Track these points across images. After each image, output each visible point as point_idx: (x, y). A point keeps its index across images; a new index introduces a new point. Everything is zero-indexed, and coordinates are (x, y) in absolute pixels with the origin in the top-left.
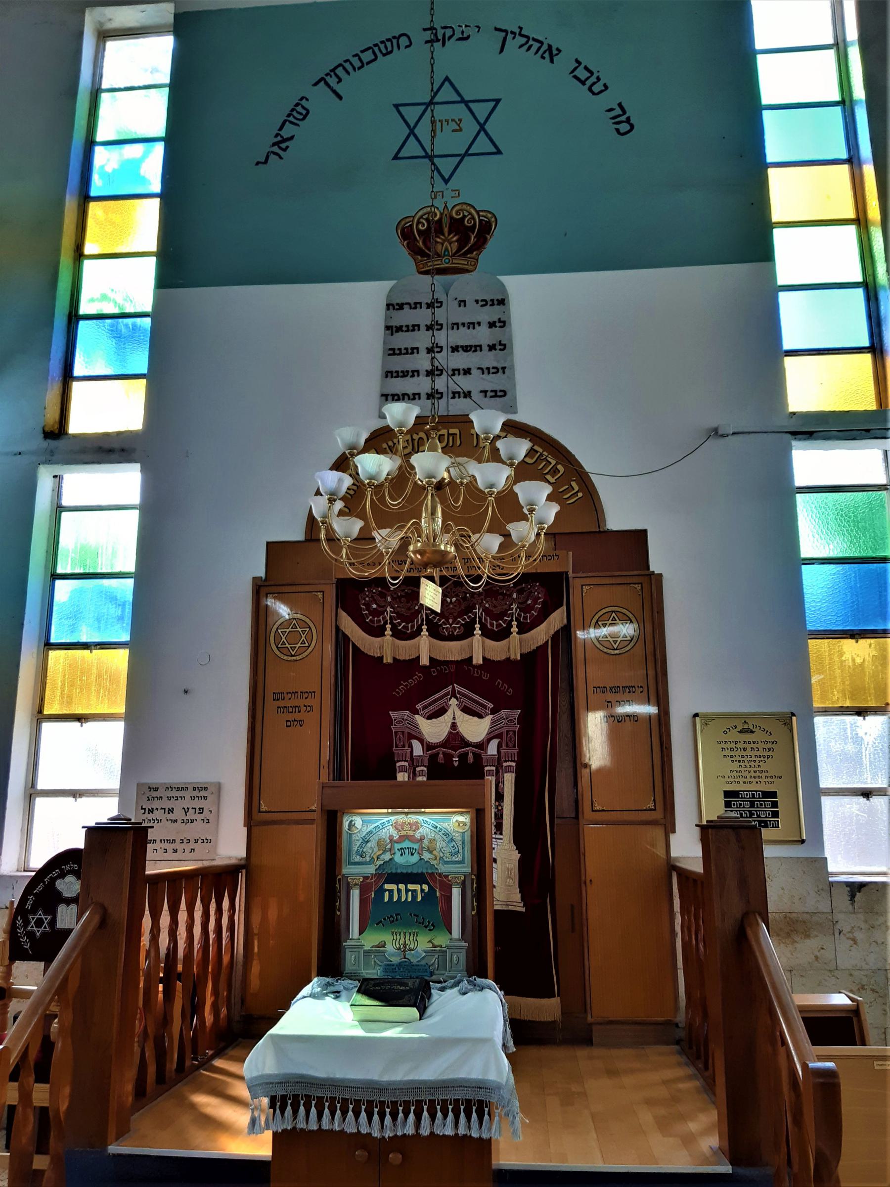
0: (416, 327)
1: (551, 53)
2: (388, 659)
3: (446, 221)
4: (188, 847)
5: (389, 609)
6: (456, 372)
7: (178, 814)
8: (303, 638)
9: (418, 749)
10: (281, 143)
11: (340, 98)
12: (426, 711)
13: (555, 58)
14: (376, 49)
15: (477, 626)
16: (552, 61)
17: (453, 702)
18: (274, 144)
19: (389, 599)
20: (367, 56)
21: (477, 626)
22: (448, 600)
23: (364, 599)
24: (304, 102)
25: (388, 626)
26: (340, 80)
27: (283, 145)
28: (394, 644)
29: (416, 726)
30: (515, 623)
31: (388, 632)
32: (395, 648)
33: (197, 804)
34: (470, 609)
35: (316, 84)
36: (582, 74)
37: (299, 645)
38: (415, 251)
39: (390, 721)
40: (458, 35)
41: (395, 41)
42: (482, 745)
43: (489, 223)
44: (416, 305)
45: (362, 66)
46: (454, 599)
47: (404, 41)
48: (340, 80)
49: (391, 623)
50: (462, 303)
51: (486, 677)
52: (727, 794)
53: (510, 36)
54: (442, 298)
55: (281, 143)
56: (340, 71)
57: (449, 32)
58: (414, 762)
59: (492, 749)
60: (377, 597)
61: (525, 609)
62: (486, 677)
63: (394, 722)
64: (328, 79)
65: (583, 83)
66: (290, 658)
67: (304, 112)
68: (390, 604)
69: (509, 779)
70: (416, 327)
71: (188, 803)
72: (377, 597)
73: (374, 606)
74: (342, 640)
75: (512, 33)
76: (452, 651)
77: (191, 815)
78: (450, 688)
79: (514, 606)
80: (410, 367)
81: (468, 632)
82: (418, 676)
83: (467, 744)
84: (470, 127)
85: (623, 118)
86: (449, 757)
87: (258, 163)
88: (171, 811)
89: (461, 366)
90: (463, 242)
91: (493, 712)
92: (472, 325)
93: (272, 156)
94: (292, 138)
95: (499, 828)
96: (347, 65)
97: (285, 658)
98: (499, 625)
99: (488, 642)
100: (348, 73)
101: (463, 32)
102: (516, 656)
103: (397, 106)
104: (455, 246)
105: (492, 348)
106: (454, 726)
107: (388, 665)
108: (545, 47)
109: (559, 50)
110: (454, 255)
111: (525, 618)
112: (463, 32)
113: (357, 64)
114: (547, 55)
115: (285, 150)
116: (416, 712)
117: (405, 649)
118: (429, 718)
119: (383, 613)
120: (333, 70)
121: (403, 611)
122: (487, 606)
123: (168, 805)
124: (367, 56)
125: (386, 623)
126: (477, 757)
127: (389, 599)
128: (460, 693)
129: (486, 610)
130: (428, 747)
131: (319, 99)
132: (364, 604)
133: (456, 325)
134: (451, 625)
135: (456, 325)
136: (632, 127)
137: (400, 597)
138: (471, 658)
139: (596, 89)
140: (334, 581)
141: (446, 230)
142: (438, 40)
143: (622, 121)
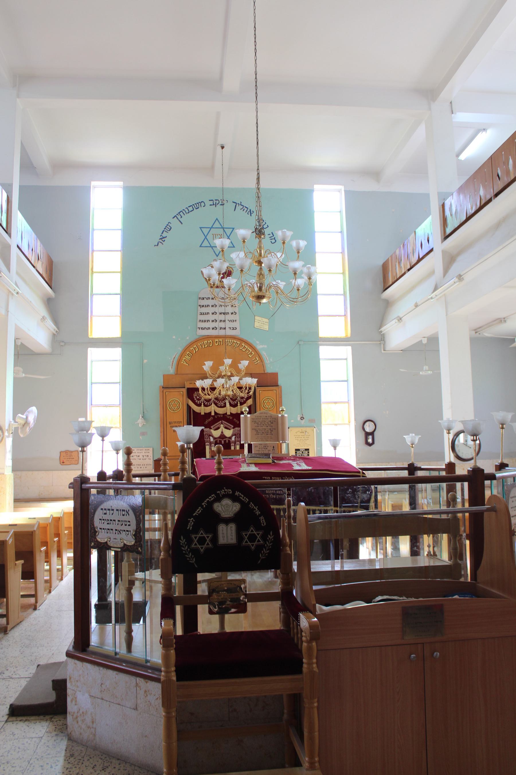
0: (208, 306)
2: (203, 413)
4: (144, 467)
6: (221, 321)
7: (141, 457)
10: (163, 238)
17: (222, 425)
20: (190, 209)
24: (169, 224)
27: (163, 240)
31: (202, 405)
32: (204, 410)
33: (147, 454)
35: (174, 218)
40: (220, 203)
42: (230, 438)
44: (208, 298)
47: (203, 204)
51: (231, 418)
52: (296, 450)
53: (237, 205)
55: (163, 238)
56: (181, 213)
57: (217, 202)
58: (211, 443)
62: (231, 418)
70: (208, 306)
76: (221, 411)
77: (145, 457)
82: (211, 418)
83: (226, 437)
88: (139, 456)
91: (233, 428)
93: (159, 243)
96: (184, 211)
99: (232, 408)
105: (232, 313)
106: (222, 432)
108: (249, 210)
113: (187, 212)
114: (249, 213)
115: (164, 241)
116: (211, 429)
117: (207, 410)
118: (215, 430)
123: (138, 454)
124: (190, 209)
126: (229, 441)
130: (215, 438)
131: (175, 223)
138: (226, 413)
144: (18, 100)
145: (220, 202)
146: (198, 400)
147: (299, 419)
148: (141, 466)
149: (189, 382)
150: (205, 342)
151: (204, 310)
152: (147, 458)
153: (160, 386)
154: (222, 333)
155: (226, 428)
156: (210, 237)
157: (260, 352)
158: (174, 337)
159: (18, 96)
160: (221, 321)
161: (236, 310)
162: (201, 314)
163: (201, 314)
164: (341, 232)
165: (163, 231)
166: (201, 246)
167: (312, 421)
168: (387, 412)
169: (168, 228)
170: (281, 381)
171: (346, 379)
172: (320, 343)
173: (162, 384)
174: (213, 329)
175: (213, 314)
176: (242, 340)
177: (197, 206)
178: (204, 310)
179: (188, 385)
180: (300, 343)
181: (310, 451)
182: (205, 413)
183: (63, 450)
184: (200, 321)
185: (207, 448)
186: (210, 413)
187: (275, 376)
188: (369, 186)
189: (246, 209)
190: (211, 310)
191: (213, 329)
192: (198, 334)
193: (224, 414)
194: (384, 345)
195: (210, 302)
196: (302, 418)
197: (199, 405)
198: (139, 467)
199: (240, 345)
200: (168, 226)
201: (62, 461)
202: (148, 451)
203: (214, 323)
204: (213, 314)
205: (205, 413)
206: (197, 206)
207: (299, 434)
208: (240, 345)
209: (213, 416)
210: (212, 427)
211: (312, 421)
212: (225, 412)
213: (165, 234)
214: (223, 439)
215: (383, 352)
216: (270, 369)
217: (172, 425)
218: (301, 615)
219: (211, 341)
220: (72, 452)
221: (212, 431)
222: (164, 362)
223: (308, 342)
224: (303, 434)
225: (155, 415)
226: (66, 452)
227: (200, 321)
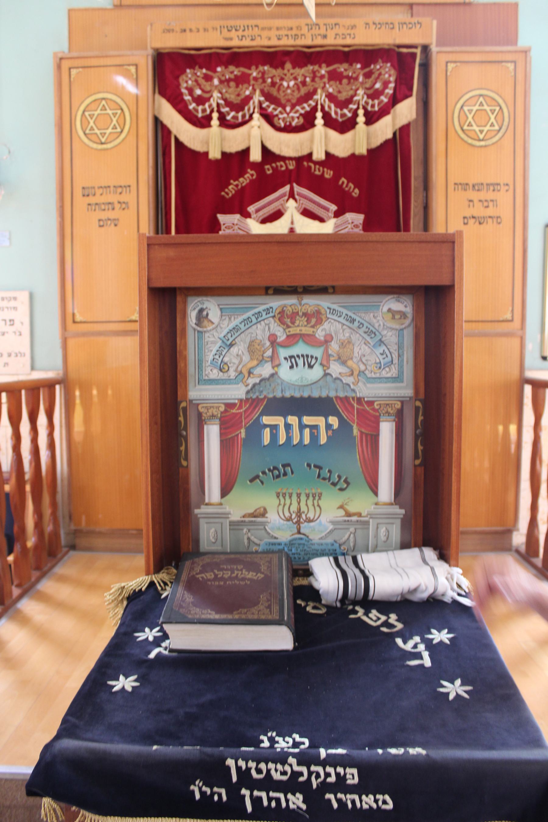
2: (215, 154)
5: (216, 94)
8: (114, 122)
12: (261, 213)
15: (319, 115)
19: (216, 82)
21: (319, 115)
22: (285, 84)
23: (187, 82)
25: (215, 115)
28: (221, 134)
30: (361, 112)
31: (215, 122)
32: (223, 139)
34: (309, 96)
37: (110, 130)
46: (292, 83)
49: (219, 111)
51: (328, 174)
60: (202, 81)
61: (374, 95)
62: (328, 174)
63: (223, 227)
66: (100, 147)
72: (202, 81)
73: (198, 92)
74: (161, 130)
76: (288, 145)
78: (287, 188)
79: (361, 92)
81: (308, 122)
82: (251, 174)
91: (337, 214)
97: (95, 146)
98: (343, 115)
99: (333, 134)
102: (362, 150)
107: (217, 161)
111: (373, 106)
116: (247, 215)
117: (234, 141)
119: (208, 99)
121: (232, 97)
122: (331, 90)
125: (212, 111)
127: (216, 82)
128: (299, 194)
129: (331, 97)
132: (187, 88)
134: (288, 114)
137: (229, 81)
138: (310, 155)
140: (150, 52)
146: (200, 101)
152: (8, 328)
155: (307, 213)
182: (224, 154)
186: (246, 152)
193: (299, 160)
197: (203, 123)
202: (13, 304)
205: (224, 154)
209: (255, 166)
210: (251, 209)
212: (305, 152)
217: (92, 200)
218: (403, 511)
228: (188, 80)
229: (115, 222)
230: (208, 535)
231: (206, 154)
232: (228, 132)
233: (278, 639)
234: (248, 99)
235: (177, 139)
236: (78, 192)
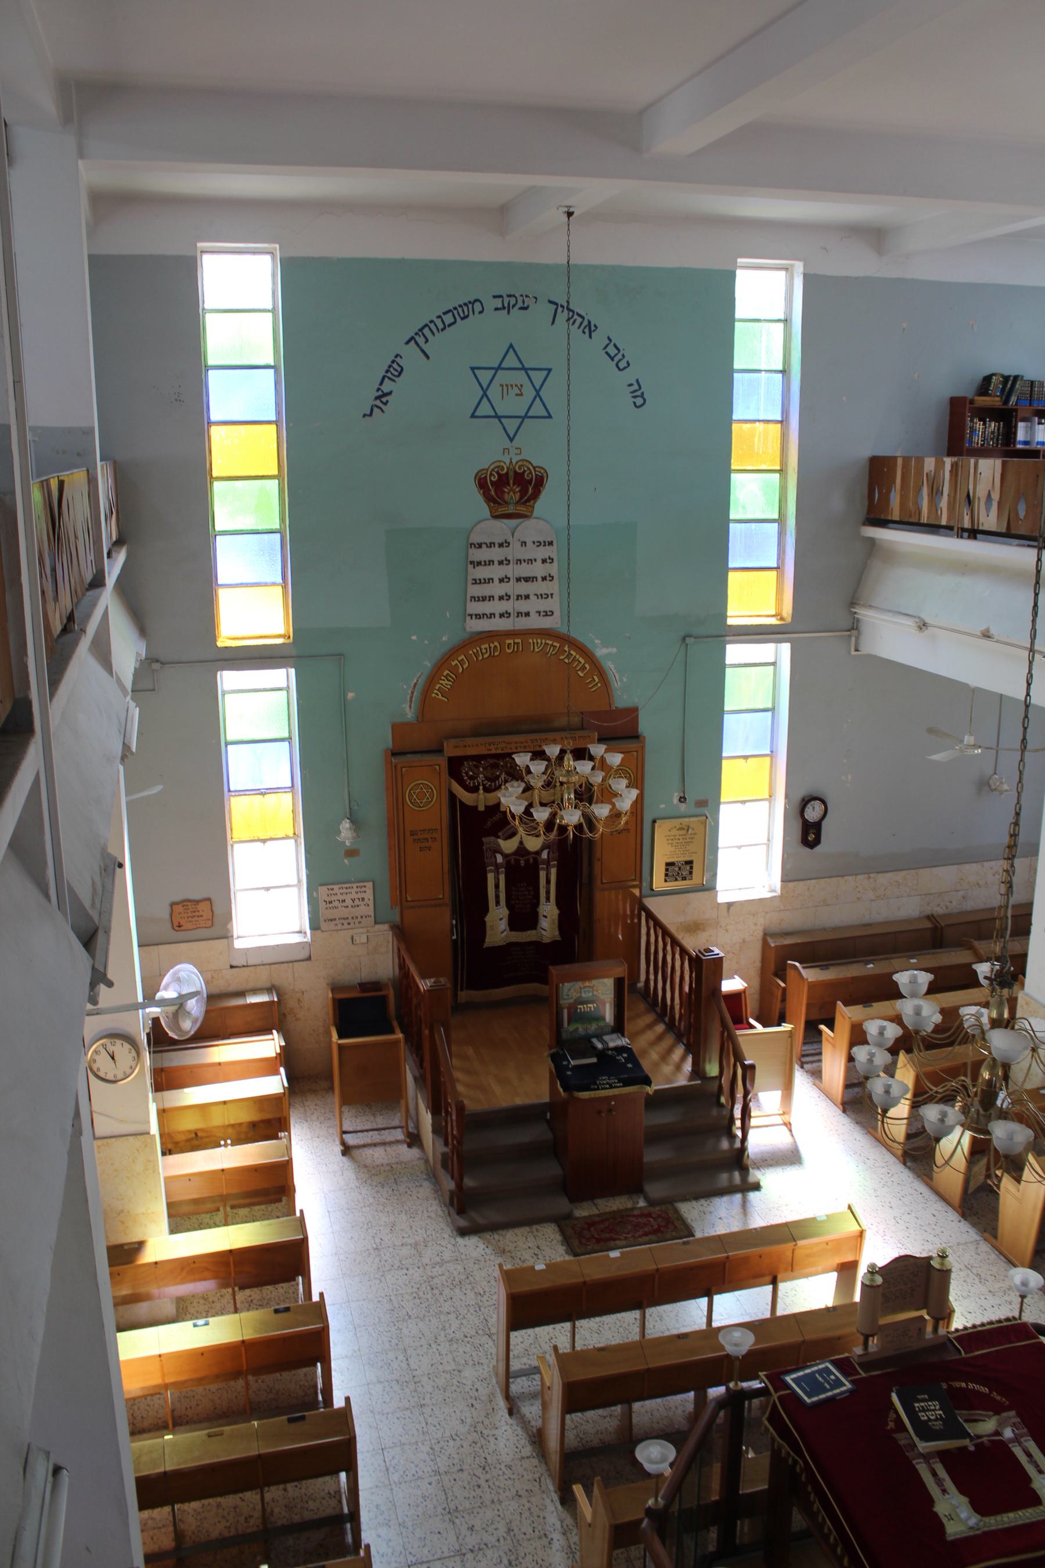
0: (491, 562)
1: (590, 329)
2: (481, 808)
3: (511, 474)
4: (357, 922)
6: (519, 597)
7: (349, 902)
9: (500, 859)
10: (382, 396)
11: (428, 357)
13: (593, 334)
14: (455, 312)
16: (590, 337)
18: (377, 398)
20: (448, 319)
24: (398, 359)
26: (427, 341)
27: (384, 400)
29: (499, 845)
31: (481, 791)
33: (360, 895)
35: (408, 343)
36: (612, 351)
38: (489, 499)
39: (482, 843)
40: (520, 304)
41: (470, 306)
42: (538, 853)
43: (542, 478)
44: (491, 545)
45: (444, 329)
47: (477, 307)
48: (427, 341)
50: (524, 544)
52: (668, 864)
53: (560, 309)
54: (510, 539)
55: (382, 396)
56: (426, 331)
57: (513, 301)
58: (497, 867)
59: (544, 855)
64: (417, 338)
65: (612, 359)
67: (399, 369)
68: (482, 773)
69: (553, 871)
70: (491, 562)
71: (354, 896)
74: (452, 797)
75: (562, 306)
77: (357, 902)
80: (487, 593)
83: (528, 853)
84: (529, 393)
85: (639, 393)
86: (517, 861)
87: (365, 416)
88: (344, 901)
89: (523, 593)
90: (523, 493)
92: (531, 561)
93: (376, 410)
94: (390, 393)
95: (548, 899)
96: (432, 326)
100: (433, 334)
101: (524, 302)
103: (473, 369)
104: (518, 495)
105: (544, 579)
106: (521, 843)
108: (586, 323)
109: (595, 326)
110: (517, 503)
112: (524, 302)
113: (440, 326)
114: (587, 330)
118: (506, 839)
120: (421, 330)
123: (341, 898)
124: (448, 319)
126: (535, 860)
130: (505, 856)
131: (411, 356)
133: (519, 561)
135: (519, 561)
136: (645, 400)
139: (622, 365)
141: (511, 482)
142: (504, 308)
143: (638, 396)
144: (80, 162)
145: (520, 300)
146: (471, 778)
147: (676, 800)
148: (350, 920)
149: (453, 741)
150: (483, 647)
151: (481, 573)
153: (386, 751)
154: (523, 624)
156: (494, 392)
157: (603, 664)
158: (414, 638)
159: (81, 154)
160: (519, 597)
161: (553, 569)
162: (475, 582)
163: (475, 582)
164: (783, 372)
165: (384, 378)
166: (473, 416)
167: (702, 803)
168: (850, 777)
169: (394, 370)
170: (645, 726)
171: (770, 706)
172: (728, 638)
173: (390, 745)
174: (502, 615)
175: (501, 581)
176: (565, 639)
177: (464, 311)
178: (481, 573)
179: (452, 749)
180: (688, 640)
181: (695, 865)
183: (177, 899)
184: (473, 598)
185: (491, 877)
187: (632, 713)
188: (858, 263)
189: (579, 320)
190: (496, 572)
191: (502, 615)
192: (468, 629)
194: (857, 638)
195: (496, 554)
196: (682, 799)
197: (474, 790)
198: (345, 922)
199: (561, 651)
200: (395, 365)
201: (176, 924)
203: (504, 602)
204: (501, 581)
206: (464, 311)
207: (675, 832)
208: (561, 651)
210: (500, 834)
211: (702, 803)
213: (387, 386)
214: (522, 856)
215: (853, 653)
216: (622, 700)
217: (416, 837)
219: (496, 643)
220: (197, 902)
221: (500, 841)
222: (392, 694)
223: (706, 634)
224: (684, 832)
225: (376, 812)
226: (184, 902)
227: (473, 598)
228: (465, 768)
229: (429, 848)
230: (564, 1036)
231: (476, 807)
232: (489, 795)
233: (594, 1060)
234: (499, 776)
235: (460, 801)
236: (408, 834)
